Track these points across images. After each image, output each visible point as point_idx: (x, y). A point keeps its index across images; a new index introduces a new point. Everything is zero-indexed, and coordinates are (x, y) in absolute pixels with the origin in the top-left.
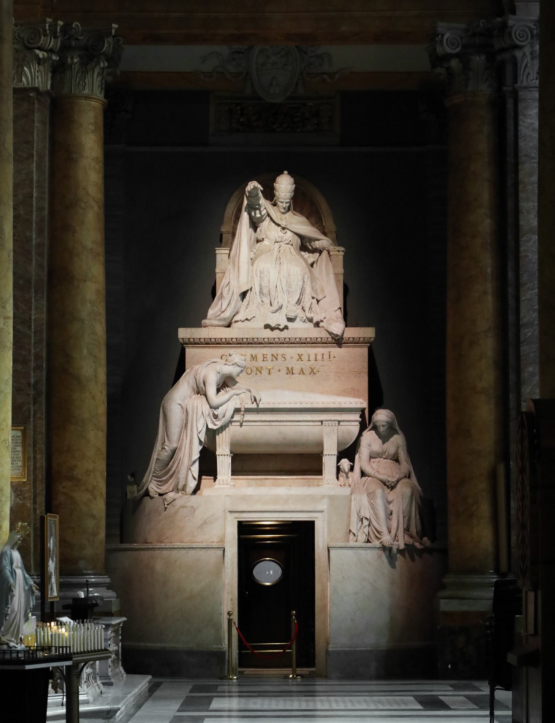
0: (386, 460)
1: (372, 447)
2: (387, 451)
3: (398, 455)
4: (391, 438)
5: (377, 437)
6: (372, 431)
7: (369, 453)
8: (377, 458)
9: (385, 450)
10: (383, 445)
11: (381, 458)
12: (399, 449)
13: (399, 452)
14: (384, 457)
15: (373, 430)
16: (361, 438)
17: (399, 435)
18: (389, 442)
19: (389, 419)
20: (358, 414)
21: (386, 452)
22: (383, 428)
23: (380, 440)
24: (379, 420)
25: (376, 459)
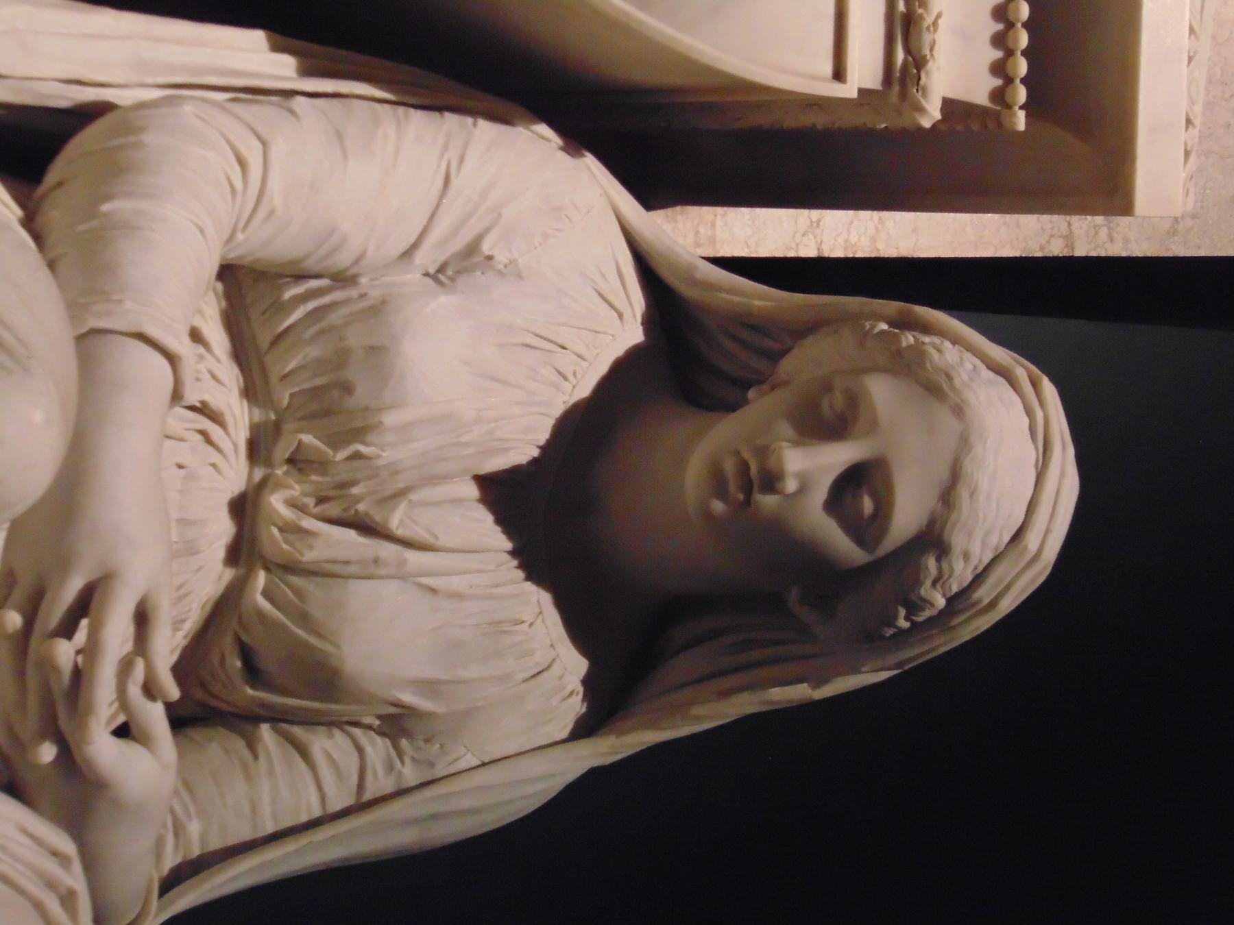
0: (223, 529)
1: (443, 301)
2: (387, 550)
3: (277, 718)
4: (563, 604)
5: (584, 389)
6: (636, 301)
7: (343, 259)
8: (250, 392)
9: (397, 521)
10: (472, 491)
11: (257, 449)
12: (377, 748)
13: (322, 743)
14: (277, 502)
15: (650, 322)
16: (819, 127)
17: (584, 729)
18: (511, 571)
19: (961, 574)
20: (998, 69)
21: (367, 528)
22: (820, 493)
23: (543, 436)
24: (959, 411)
25: (230, 374)
